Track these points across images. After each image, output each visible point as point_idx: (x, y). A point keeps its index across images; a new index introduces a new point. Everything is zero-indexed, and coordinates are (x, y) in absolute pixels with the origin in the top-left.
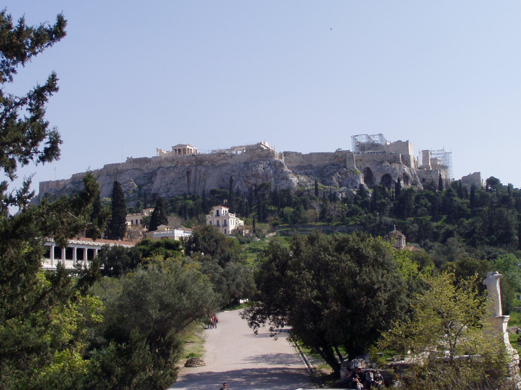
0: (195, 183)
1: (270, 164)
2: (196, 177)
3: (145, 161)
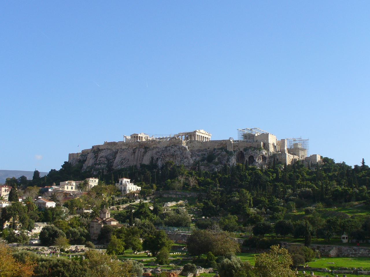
1: (179, 148)
2: (138, 155)
3: (114, 144)
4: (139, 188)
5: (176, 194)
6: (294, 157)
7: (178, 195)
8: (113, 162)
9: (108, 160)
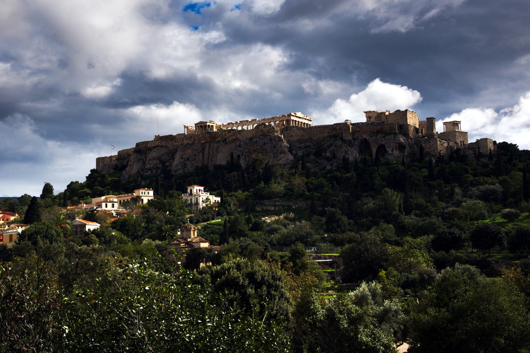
0: (208, 159)
2: (209, 153)
4: (219, 199)
5: (275, 206)
6: (448, 144)
7: (278, 206)
8: (171, 165)
9: (163, 163)
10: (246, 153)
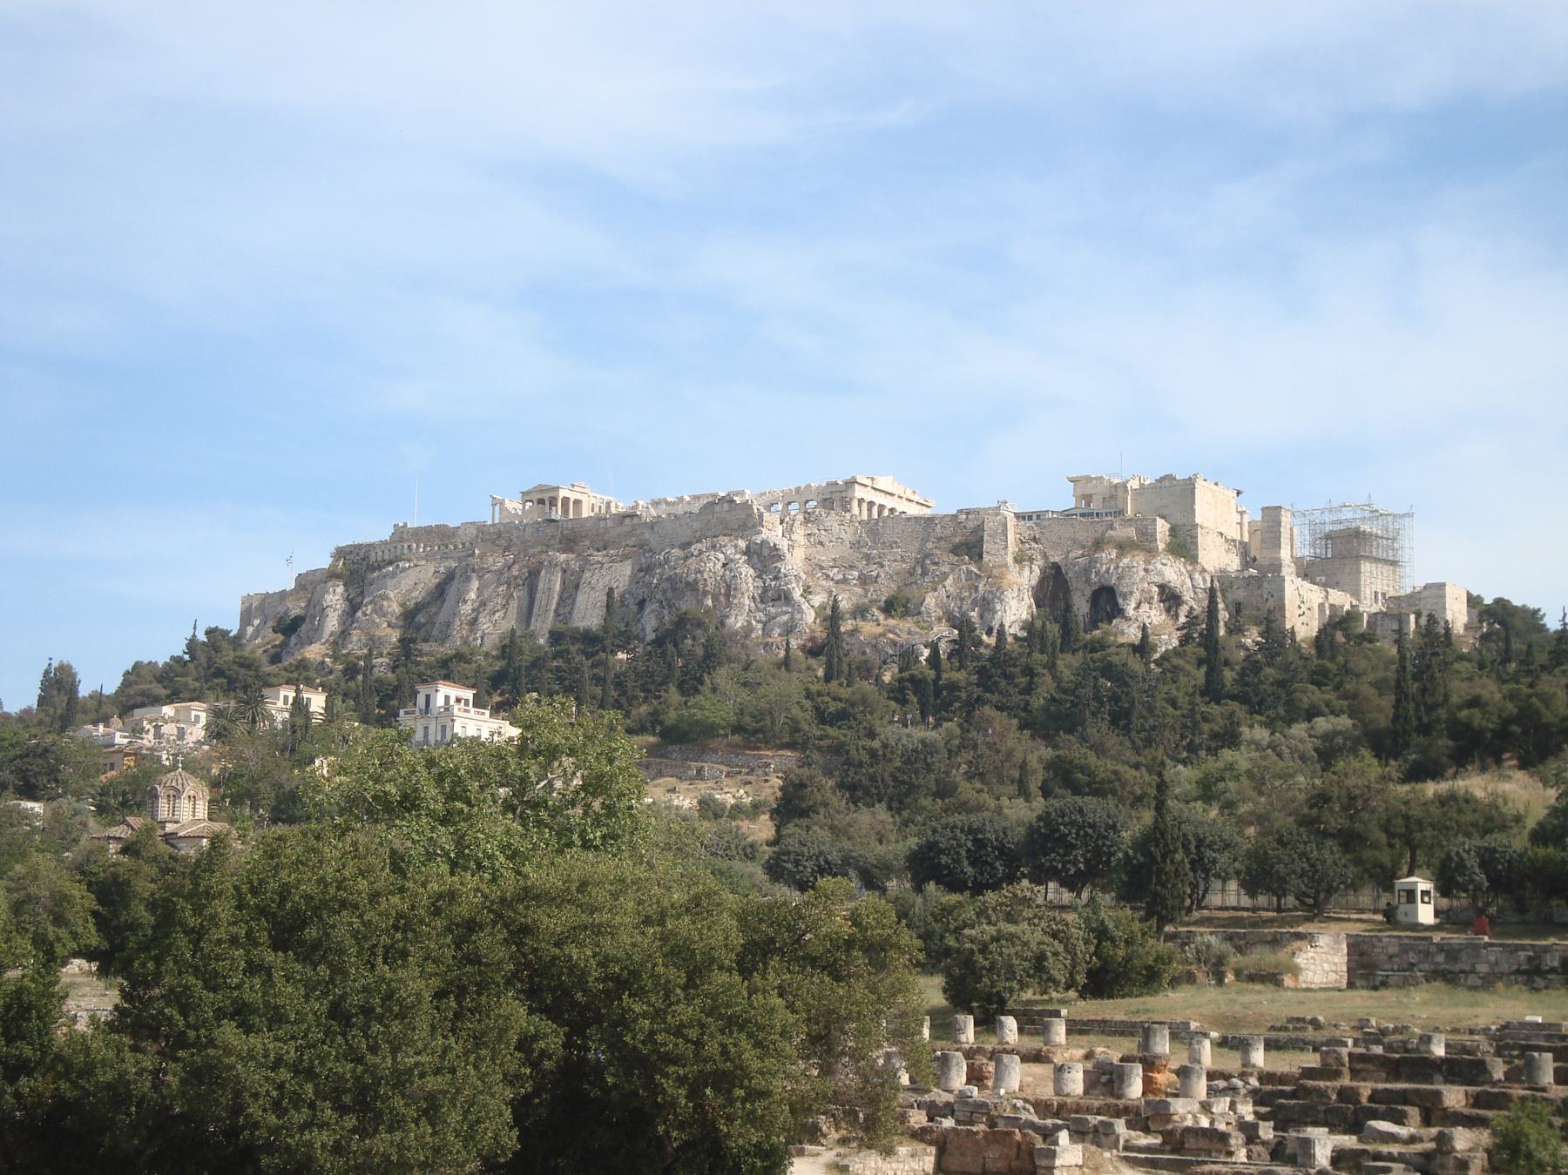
10: (664, 592)
